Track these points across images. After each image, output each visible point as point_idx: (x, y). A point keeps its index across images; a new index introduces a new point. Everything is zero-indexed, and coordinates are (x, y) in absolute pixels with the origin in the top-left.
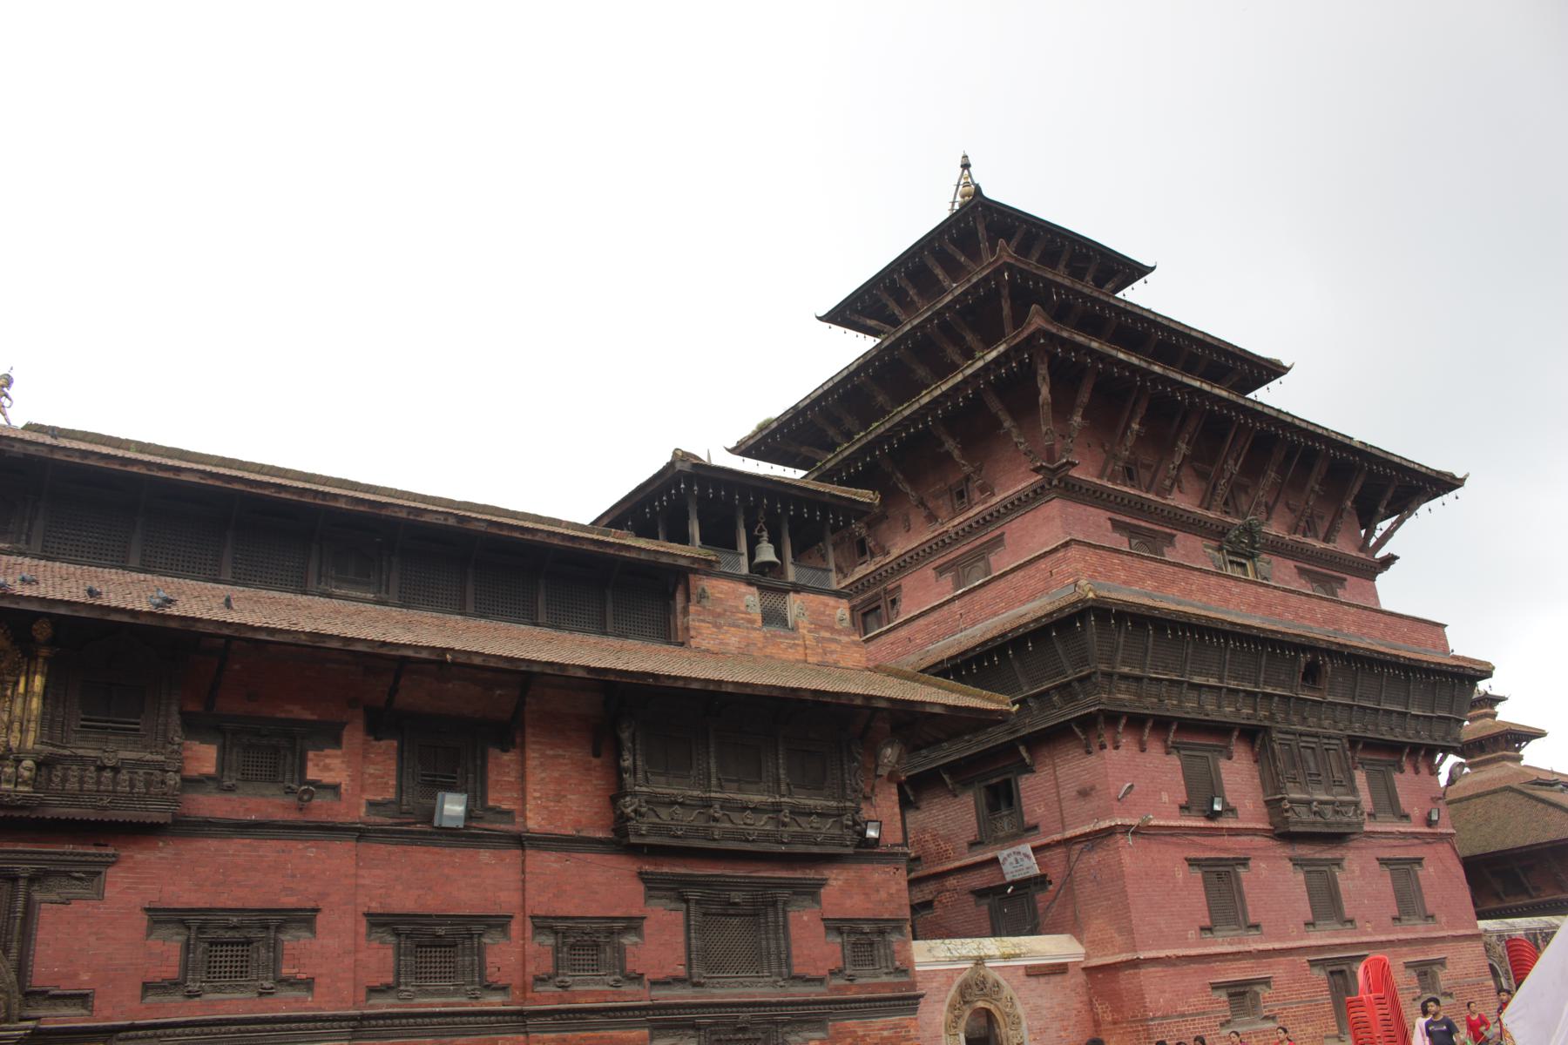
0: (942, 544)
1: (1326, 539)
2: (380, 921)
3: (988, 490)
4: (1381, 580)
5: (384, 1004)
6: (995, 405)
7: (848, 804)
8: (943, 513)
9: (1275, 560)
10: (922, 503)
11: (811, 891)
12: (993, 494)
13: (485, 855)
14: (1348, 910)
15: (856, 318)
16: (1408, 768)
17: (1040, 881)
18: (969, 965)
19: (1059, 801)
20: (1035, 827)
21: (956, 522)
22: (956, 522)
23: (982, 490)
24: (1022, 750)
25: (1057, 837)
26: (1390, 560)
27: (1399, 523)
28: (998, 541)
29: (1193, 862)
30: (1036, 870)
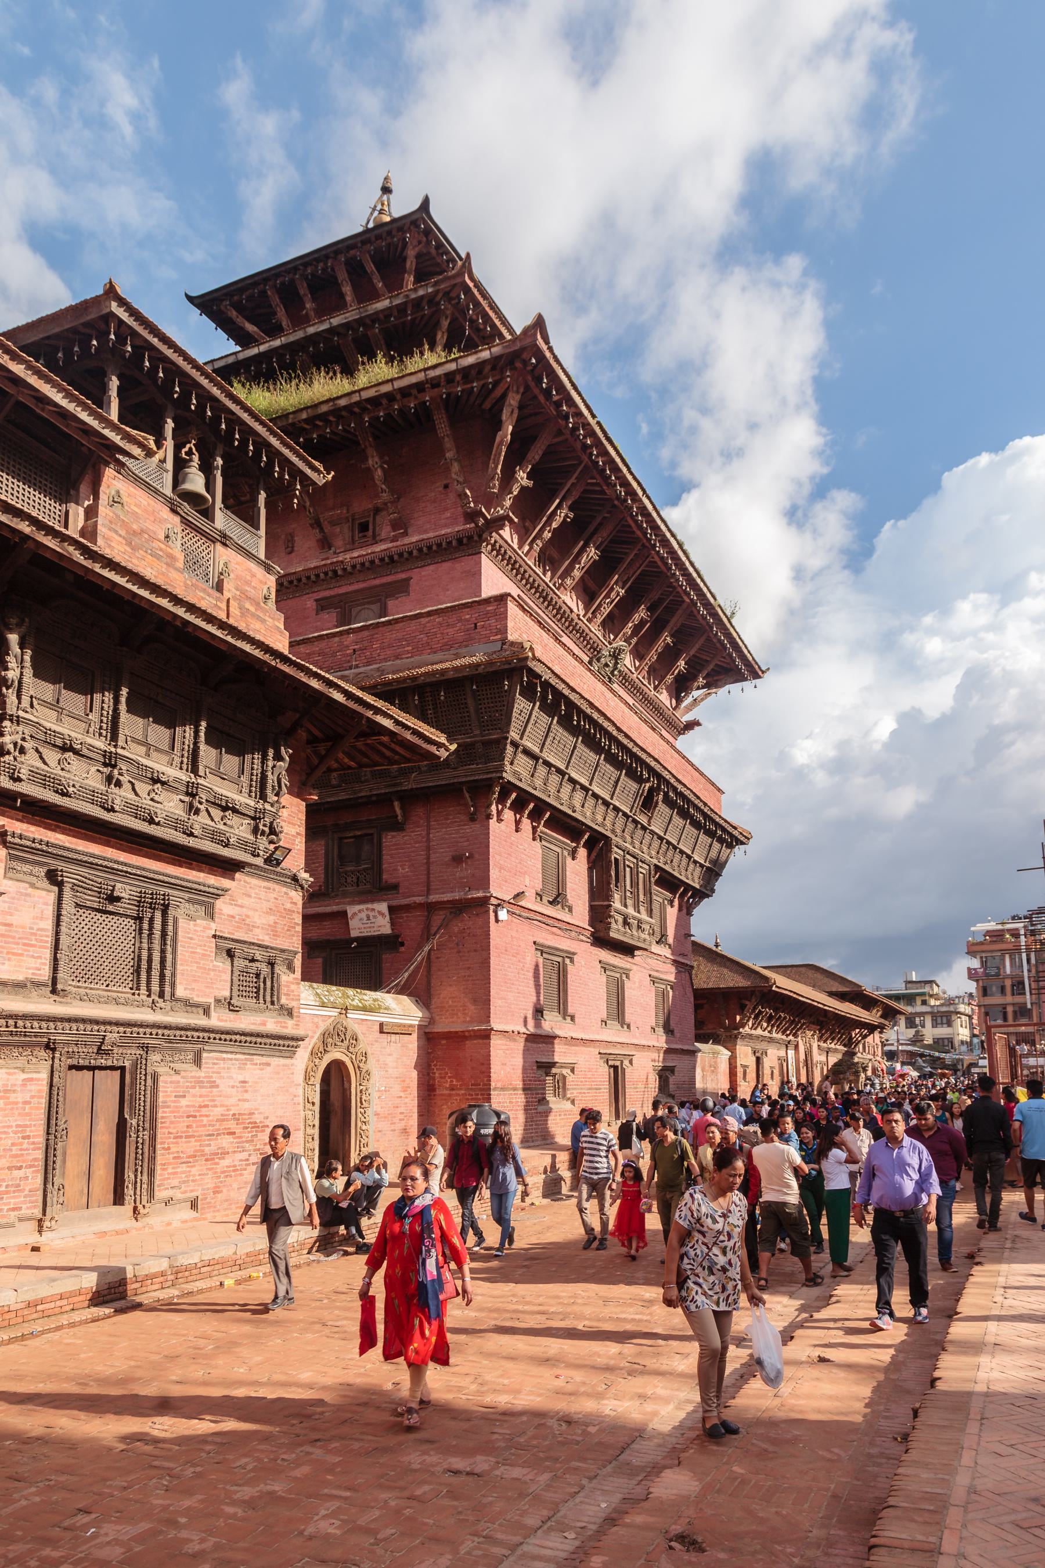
0: (334, 575)
7: (268, 806)
8: (339, 542)
10: (317, 524)
11: (206, 901)
12: (406, 534)
15: (233, 314)
18: (334, 1013)
19: (428, 864)
20: (395, 887)
21: (355, 554)
22: (355, 554)
23: (395, 526)
24: (396, 804)
25: (419, 899)
29: (541, 949)
30: (387, 930)
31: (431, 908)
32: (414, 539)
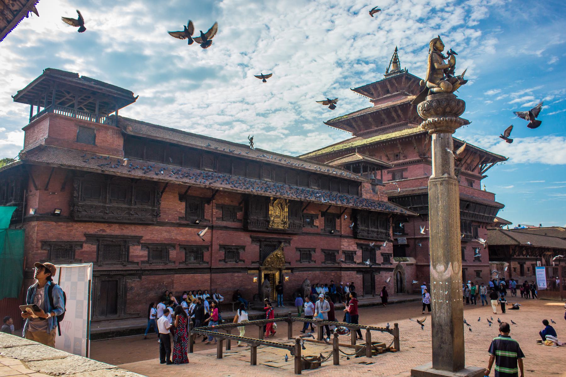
1: (473, 171)
2: (323, 250)
3: (405, 157)
4: (482, 181)
5: (324, 265)
6: (414, 141)
9: (462, 176)
13: (336, 239)
14: (465, 259)
16: (481, 228)
17: (408, 246)
20: (407, 234)
23: (404, 157)
25: (413, 237)
26: (486, 176)
27: (490, 166)
28: (406, 169)
31: (416, 239)
32: (408, 160)
